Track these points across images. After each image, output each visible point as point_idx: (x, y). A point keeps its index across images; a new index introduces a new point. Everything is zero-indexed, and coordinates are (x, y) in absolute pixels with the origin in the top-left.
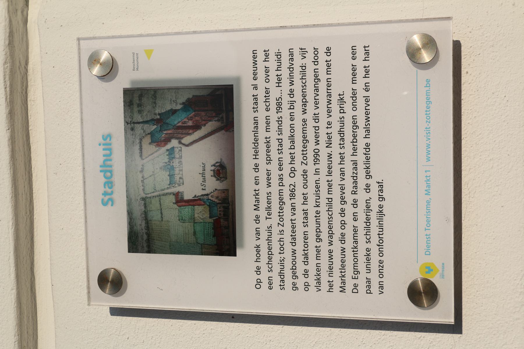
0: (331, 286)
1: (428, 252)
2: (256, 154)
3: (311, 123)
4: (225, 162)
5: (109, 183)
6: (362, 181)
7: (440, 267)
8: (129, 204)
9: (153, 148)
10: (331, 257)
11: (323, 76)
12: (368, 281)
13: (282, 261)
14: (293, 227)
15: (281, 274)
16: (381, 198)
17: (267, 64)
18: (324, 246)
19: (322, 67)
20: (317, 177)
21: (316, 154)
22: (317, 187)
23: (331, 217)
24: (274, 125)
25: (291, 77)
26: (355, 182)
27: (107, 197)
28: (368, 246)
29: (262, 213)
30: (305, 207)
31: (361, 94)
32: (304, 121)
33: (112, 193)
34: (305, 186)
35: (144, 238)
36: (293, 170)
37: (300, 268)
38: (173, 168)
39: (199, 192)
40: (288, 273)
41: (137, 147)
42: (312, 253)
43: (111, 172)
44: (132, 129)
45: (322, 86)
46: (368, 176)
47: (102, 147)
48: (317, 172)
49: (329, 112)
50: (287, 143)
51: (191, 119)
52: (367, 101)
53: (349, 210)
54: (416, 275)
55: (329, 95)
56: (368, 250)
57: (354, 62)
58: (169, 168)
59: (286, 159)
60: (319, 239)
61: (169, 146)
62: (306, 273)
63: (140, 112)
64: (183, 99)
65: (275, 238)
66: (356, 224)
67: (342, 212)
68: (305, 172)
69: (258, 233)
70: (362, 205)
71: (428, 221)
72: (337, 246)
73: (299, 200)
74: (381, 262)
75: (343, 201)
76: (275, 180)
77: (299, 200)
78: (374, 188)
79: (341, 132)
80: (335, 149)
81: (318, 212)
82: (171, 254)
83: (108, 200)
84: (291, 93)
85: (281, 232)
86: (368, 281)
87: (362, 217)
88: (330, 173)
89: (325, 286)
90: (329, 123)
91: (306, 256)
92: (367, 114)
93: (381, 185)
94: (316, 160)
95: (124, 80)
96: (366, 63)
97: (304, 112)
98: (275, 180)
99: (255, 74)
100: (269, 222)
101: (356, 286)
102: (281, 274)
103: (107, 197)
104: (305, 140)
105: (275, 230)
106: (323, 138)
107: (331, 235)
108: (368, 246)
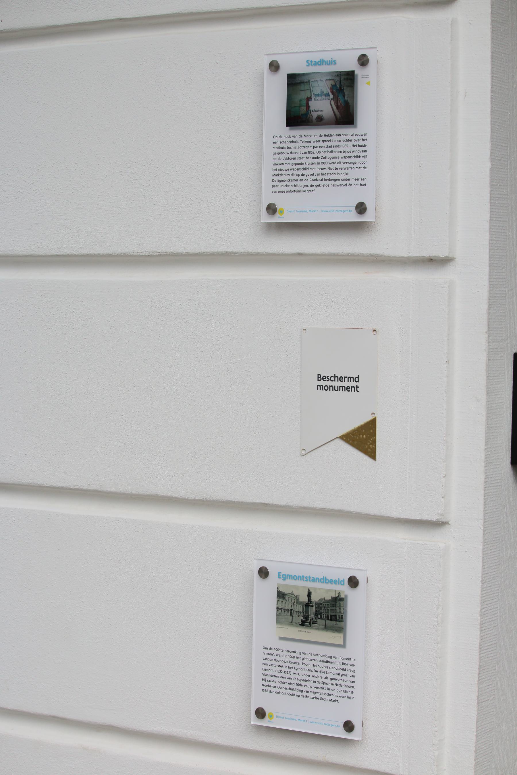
0: (275, 170)
1: (288, 211)
2: (326, 136)
3: (337, 160)
4: (323, 121)
5: (316, 64)
6: (315, 183)
7: (282, 217)
8: (307, 74)
9: (330, 86)
10: (286, 170)
11: (356, 166)
12: (277, 186)
13: (284, 148)
14: (297, 153)
15: (279, 148)
16: (308, 192)
17: (361, 140)
18: (290, 167)
19: (359, 165)
20: (316, 163)
21: (325, 163)
22: (312, 164)
23: (301, 169)
24: (337, 144)
25: (356, 151)
26: (314, 180)
27: (310, 63)
28: (290, 186)
29: (303, 139)
30: (305, 158)
31: (348, 182)
32: (338, 158)
33: (312, 65)
34: (313, 158)
35: (294, 81)
36: (319, 153)
37: (282, 156)
38: (321, 96)
39: (311, 109)
40: (280, 151)
41: (330, 78)
42: (288, 161)
43: (321, 64)
44: (338, 75)
45: (352, 166)
46: (317, 186)
47: (331, 60)
48: (319, 163)
49: (342, 169)
50: (330, 149)
51: (341, 104)
52: (345, 185)
53: (304, 178)
54: (278, 207)
55: (348, 169)
56: (289, 186)
57: (360, 180)
58: (322, 94)
59: (324, 149)
60: (293, 164)
61: (330, 94)
62: (280, 159)
63: (345, 79)
64: (349, 101)
65: (293, 145)
66: (299, 180)
67: (303, 175)
68: (319, 158)
69: (295, 137)
70: (305, 183)
71: (299, 211)
72: (290, 172)
73: (308, 155)
74: (284, 192)
75: (307, 175)
76: (316, 144)
77: (308, 155)
78: (312, 189)
79: (333, 174)
80: (327, 171)
81: (303, 164)
82: (287, 95)
83: (309, 63)
84: (349, 152)
85: (296, 147)
86: (277, 186)
87: (301, 183)
88: (318, 169)
89: (275, 167)
90: (337, 169)
91: (286, 159)
92: (340, 185)
93: (313, 191)
94: (324, 163)
95: (359, 72)
96: (359, 185)
97: (342, 158)
98: (316, 144)
99: (357, 135)
100: (299, 142)
101: (275, 181)
102: (279, 148)
103: (310, 63)
104: (331, 158)
105: (296, 145)
106: (331, 166)
107: (294, 170)
108: (290, 186)
